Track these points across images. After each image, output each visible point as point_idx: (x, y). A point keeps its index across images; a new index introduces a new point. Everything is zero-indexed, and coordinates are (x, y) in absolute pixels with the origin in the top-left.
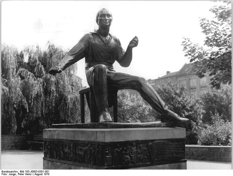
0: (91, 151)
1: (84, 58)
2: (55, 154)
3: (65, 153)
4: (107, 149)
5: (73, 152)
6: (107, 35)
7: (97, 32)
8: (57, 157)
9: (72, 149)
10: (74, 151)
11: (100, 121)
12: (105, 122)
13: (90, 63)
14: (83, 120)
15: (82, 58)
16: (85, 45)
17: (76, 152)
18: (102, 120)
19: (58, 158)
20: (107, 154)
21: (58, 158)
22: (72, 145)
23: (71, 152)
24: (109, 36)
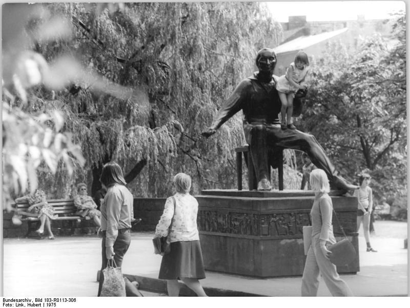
0: (247, 220)
1: (242, 110)
2: (207, 227)
3: (219, 224)
4: (263, 218)
5: (228, 223)
6: (271, 80)
7: (257, 78)
8: (209, 228)
9: (227, 219)
10: (229, 222)
11: (258, 189)
12: (263, 190)
13: (248, 119)
14: (240, 187)
15: (240, 110)
16: (241, 95)
17: (231, 222)
18: (260, 187)
19: (211, 230)
20: (263, 224)
21: (211, 230)
22: (226, 215)
23: (226, 222)
24: (273, 81)
